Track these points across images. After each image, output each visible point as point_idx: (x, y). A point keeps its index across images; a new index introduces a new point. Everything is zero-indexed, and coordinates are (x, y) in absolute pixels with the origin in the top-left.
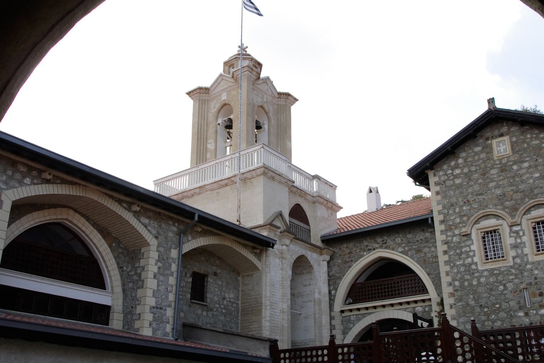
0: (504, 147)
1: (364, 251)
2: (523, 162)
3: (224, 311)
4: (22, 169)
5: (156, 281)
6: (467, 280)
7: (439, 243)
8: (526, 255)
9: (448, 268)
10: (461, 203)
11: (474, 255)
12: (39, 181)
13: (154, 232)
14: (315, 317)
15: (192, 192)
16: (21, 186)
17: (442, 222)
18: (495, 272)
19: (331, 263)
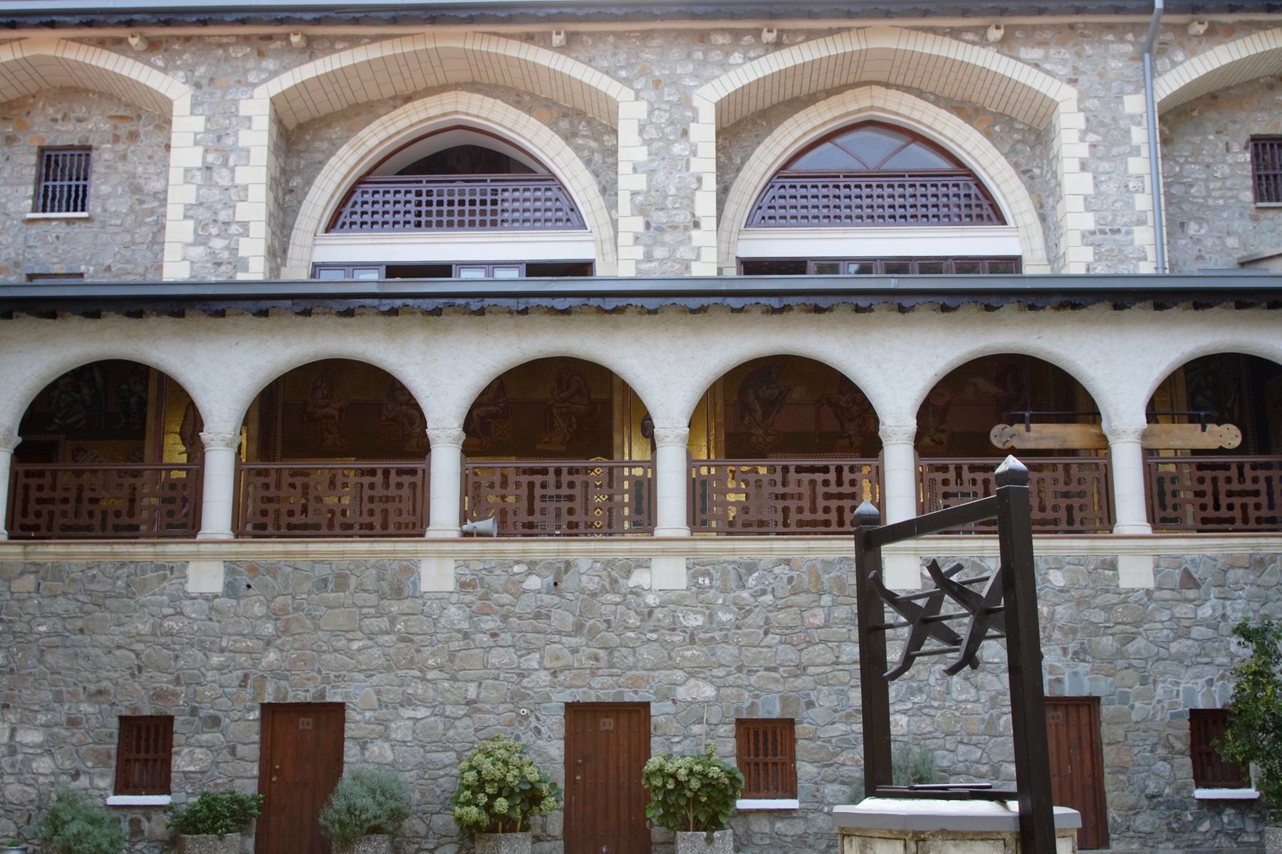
4: (720, 40)
5: (1088, 177)
12: (760, 51)
13: (1062, 73)
16: (726, 71)
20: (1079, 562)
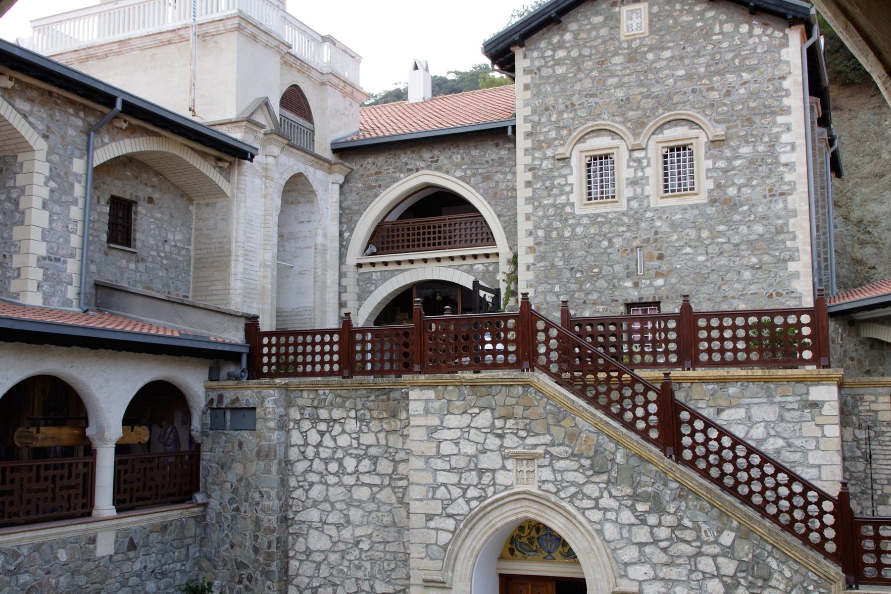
0: (638, 20)
1: (401, 171)
2: (663, 49)
3: (165, 262)
6: (556, 229)
7: (520, 169)
8: (648, 197)
9: (529, 209)
10: (562, 107)
11: (572, 192)
14: (315, 273)
15: (106, 49)
17: (529, 135)
18: (599, 219)
19: (346, 187)
20: (77, 540)
